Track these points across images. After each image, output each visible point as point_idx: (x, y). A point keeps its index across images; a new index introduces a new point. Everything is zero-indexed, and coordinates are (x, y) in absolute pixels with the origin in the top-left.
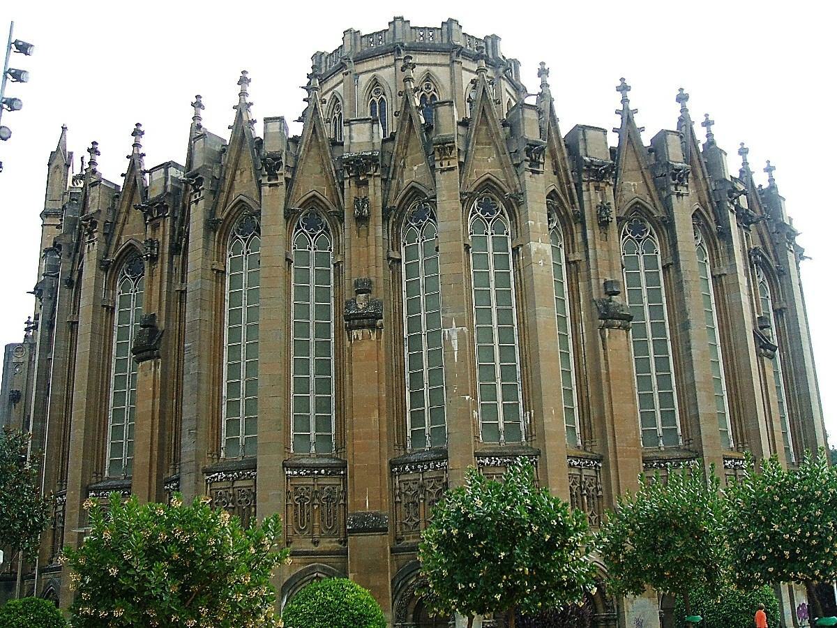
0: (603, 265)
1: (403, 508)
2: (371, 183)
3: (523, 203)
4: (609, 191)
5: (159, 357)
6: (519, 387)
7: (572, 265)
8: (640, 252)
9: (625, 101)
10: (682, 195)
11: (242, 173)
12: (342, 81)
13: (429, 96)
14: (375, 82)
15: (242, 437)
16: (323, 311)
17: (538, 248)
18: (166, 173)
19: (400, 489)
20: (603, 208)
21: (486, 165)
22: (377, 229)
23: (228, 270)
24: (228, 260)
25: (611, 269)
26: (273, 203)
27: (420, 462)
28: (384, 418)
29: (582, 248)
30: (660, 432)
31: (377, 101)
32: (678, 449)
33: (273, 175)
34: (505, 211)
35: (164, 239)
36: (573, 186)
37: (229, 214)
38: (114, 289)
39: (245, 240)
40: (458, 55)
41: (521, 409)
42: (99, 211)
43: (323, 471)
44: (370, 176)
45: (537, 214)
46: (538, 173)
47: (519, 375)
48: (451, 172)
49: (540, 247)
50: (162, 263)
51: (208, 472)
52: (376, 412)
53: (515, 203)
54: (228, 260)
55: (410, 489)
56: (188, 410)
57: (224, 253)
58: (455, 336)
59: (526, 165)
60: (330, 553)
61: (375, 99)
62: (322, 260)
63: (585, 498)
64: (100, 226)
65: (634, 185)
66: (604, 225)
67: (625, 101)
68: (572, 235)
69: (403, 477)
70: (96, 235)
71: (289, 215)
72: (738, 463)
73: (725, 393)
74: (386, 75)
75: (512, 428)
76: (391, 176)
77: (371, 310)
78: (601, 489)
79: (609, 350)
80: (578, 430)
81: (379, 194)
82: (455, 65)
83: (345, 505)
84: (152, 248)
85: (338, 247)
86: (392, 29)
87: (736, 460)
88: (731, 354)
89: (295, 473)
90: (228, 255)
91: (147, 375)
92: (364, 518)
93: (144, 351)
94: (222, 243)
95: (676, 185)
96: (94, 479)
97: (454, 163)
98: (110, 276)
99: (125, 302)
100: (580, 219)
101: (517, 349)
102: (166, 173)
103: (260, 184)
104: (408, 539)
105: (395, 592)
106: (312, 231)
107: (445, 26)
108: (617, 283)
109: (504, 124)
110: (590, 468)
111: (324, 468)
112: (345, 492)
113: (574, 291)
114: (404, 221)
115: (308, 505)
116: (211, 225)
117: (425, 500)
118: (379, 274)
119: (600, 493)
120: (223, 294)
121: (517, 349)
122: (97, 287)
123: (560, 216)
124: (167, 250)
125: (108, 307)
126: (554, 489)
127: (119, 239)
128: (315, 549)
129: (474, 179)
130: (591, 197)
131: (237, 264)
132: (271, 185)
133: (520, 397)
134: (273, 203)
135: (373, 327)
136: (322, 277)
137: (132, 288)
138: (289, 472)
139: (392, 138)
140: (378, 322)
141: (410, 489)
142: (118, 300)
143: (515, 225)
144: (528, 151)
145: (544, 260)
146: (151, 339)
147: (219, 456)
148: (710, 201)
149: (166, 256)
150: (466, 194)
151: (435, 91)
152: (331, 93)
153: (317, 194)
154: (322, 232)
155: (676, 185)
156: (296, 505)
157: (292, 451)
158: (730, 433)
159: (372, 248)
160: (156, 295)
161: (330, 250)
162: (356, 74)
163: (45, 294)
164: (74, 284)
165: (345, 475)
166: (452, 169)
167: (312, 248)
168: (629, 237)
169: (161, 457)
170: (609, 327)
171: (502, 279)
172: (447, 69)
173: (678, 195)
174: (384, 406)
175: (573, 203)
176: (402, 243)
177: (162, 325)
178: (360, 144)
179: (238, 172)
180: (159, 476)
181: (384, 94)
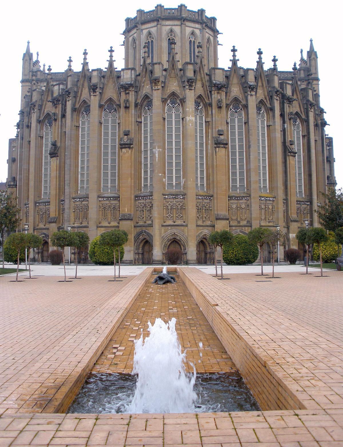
1: (139, 212)
2: (131, 93)
3: (185, 101)
4: (223, 94)
5: (58, 156)
6: (182, 170)
7: (207, 123)
8: (236, 117)
9: (234, 56)
10: (253, 95)
11: (85, 89)
12: (136, 33)
13: (171, 39)
14: (150, 33)
15: (85, 186)
16: (113, 140)
17: (190, 119)
18: (59, 87)
19: (138, 205)
20: (220, 101)
21: (174, 86)
22: (132, 110)
23: (81, 125)
24: (81, 122)
26: (94, 101)
27: (145, 196)
28: (133, 181)
29: (211, 116)
30: (238, 186)
31: (150, 41)
32: (244, 193)
33: (94, 91)
34: (180, 104)
35: (59, 112)
36: (209, 92)
37: (80, 105)
38: (43, 130)
39: (86, 114)
40: (184, 21)
41: (182, 178)
42: (36, 101)
43: (112, 199)
44: (130, 91)
45: (190, 105)
46: (192, 90)
47: (181, 166)
50: (58, 121)
51: (74, 199)
52: (130, 179)
53: (183, 101)
54: (81, 122)
55: (141, 206)
56: (67, 177)
57: (79, 120)
58: (157, 152)
59: (187, 87)
60: (114, 227)
61: (149, 40)
62: (114, 121)
63: (204, 210)
64: (37, 107)
65: (236, 90)
66: (220, 107)
67: (234, 56)
68: (208, 111)
69: (139, 201)
70: (35, 110)
71: (101, 106)
72: (267, 199)
73: (267, 171)
74: (154, 30)
75: (178, 184)
76: (138, 90)
77: (128, 142)
78: (211, 207)
80: (205, 185)
81: (133, 97)
82: (183, 25)
83: (119, 210)
84: (55, 116)
85: (119, 117)
86: (156, 10)
87: (266, 197)
88: (271, 157)
89: (102, 199)
90: (80, 120)
91: (54, 162)
92: (124, 215)
93: (53, 154)
94: (78, 116)
95: (250, 91)
96: (38, 199)
97: (159, 87)
98: (41, 126)
99: (47, 134)
100: (210, 105)
101: (181, 156)
102: (59, 87)
103: (90, 95)
104: (140, 223)
105: (135, 241)
106: (110, 111)
107: (179, 8)
108: (223, 131)
109: (181, 70)
110: (207, 199)
111: (112, 198)
112: (119, 206)
113: (207, 132)
114: (143, 107)
115: (107, 210)
116: (74, 110)
117: (146, 210)
118: (132, 128)
119: (211, 208)
120: (79, 135)
121: (181, 156)
122: (36, 130)
123: (203, 103)
124: (60, 116)
125: (41, 137)
126: (190, 207)
127: (44, 111)
128: (108, 225)
129: (169, 91)
130: (216, 96)
131: (83, 123)
132: (94, 96)
133: (182, 173)
134: (94, 101)
135: (129, 148)
136: (114, 128)
137: (49, 129)
138: (100, 199)
139: (139, 75)
140: (132, 146)
141: (141, 206)
142: (44, 134)
143: (183, 109)
144: (188, 82)
145: (192, 124)
146: (55, 150)
147: (77, 192)
148: (268, 96)
149: (60, 119)
150: (164, 99)
151: (174, 36)
152: (132, 36)
153: (111, 97)
154: (114, 111)
155: (250, 91)
156: (103, 210)
157: (102, 191)
158: (268, 187)
159: (130, 118)
160: (56, 134)
161: (117, 118)
162: (142, 30)
163: (21, 126)
164: (29, 127)
165: (119, 200)
166: (158, 89)
167: (110, 117)
169: (59, 192)
170: (218, 147)
171: (177, 130)
172: (179, 27)
173: (251, 95)
174: (133, 176)
175: (209, 98)
176: (142, 115)
177: (58, 144)
178: (127, 78)
179: (84, 89)
180: (59, 199)
181: (153, 38)
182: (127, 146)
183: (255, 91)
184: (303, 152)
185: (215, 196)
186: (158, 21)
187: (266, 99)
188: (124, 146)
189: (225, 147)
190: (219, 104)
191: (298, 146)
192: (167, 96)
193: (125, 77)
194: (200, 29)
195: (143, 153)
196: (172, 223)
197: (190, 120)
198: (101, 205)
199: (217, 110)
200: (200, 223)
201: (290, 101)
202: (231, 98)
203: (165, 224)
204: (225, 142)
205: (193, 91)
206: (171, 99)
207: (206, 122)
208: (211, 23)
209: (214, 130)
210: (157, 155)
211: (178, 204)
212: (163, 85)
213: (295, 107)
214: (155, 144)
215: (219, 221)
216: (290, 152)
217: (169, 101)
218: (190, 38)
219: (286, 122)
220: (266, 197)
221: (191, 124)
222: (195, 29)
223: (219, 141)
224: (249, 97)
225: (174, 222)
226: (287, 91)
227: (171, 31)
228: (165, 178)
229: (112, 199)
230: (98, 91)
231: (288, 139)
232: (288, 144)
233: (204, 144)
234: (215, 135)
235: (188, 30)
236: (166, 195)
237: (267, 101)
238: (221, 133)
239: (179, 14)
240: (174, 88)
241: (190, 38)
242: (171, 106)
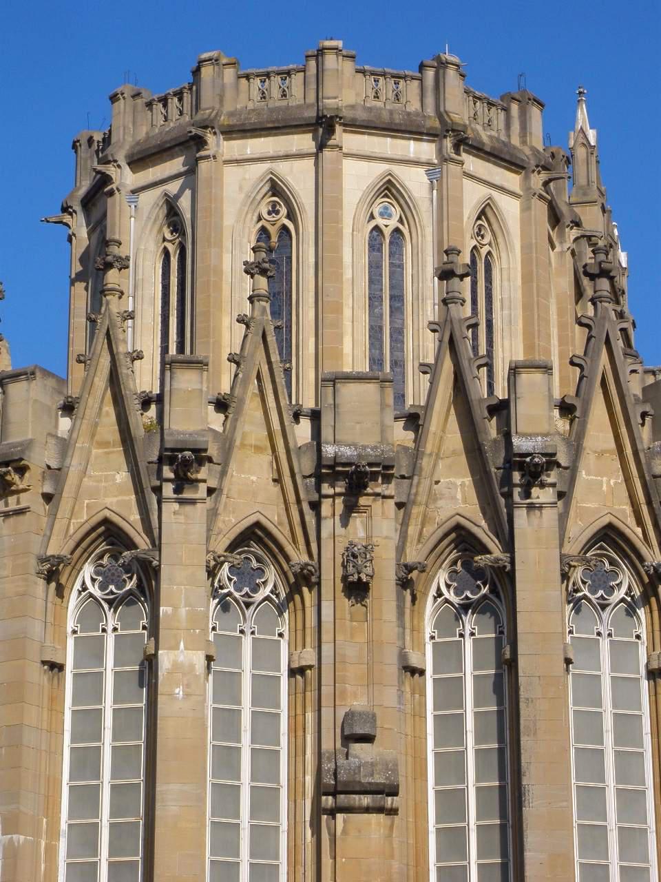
0: (353, 672)
7: (299, 677)
13: (273, 231)
25: (371, 680)
36: (306, 507)
46: (193, 502)
48: (21, 518)
49: (181, 658)
59: (168, 490)
65: (463, 485)
82: (327, 153)
109: (146, 403)
145: (188, 686)
166: (20, 512)
168: (447, 601)
183: (553, 485)
189: (380, 810)
190: (351, 569)
194: (429, 164)
197: (176, 666)
199: (345, 603)
202: (433, 532)
204: (379, 779)
205: (200, 511)
206: (101, 557)
207: (293, 672)
209: (327, 713)
212: (48, 488)
217: (88, 570)
218: (372, 217)
221: (179, 691)
222: (397, 170)
223: (343, 776)
224: (520, 516)
227: (276, 189)
238: (359, 730)
239: (311, 98)
240: (111, 501)
241: (372, 217)
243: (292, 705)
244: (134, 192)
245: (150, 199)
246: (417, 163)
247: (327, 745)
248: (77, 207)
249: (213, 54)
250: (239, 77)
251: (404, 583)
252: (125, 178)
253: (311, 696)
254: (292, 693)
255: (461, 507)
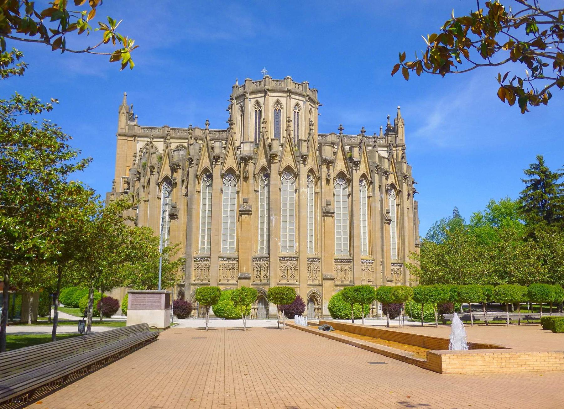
13: (278, 110)
31: (258, 110)
41: (294, 242)
58: (274, 219)
77: (247, 209)
79: (326, 224)
87: (367, 260)
127: (163, 173)
128: (228, 283)
182: (246, 212)
184: (397, 219)
185: (323, 258)
186: (266, 92)
187: (367, 173)
188: (243, 212)
191: (393, 215)
192: (283, 169)
193: (244, 149)
195: (259, 218)
196: (287, 282)
198: (221, 264)
200: (310, 282)
201: (386, 173)
203: (280, 283)
207: (315, 193)
208: (313, 94)
209: (323, 200)
210: (274, 222)
211: (291, 265)
213: (392, 179)
214: (272, 212)
215: (326, 281)
216: (386, 220)
219: (383, 193)
220: (367, 260)
222: (299, 101)
223: (327, 211)
225: (288, 281)
226: (385, 165)
228: (279, 241)
229: (231, 259)
230: (220, 161)
231: (385, 208)
232: (384, 212)
233: (314, 212)
234: (324, 204)
235: (293, 102)
236: (281, 258)
237: (368, 175)
242: (286, 178)
243: (315, 198)
244: (250, 99)
245: (253, 101)
246: (302, 101)
247: (323, 205)
248: (234, 99)
249: (268, 76)
250: (272, 81)
251: (334, 180)
252: (248, 96)
253: (319, 197)
254: (315, 196)
255: (341, 168)
